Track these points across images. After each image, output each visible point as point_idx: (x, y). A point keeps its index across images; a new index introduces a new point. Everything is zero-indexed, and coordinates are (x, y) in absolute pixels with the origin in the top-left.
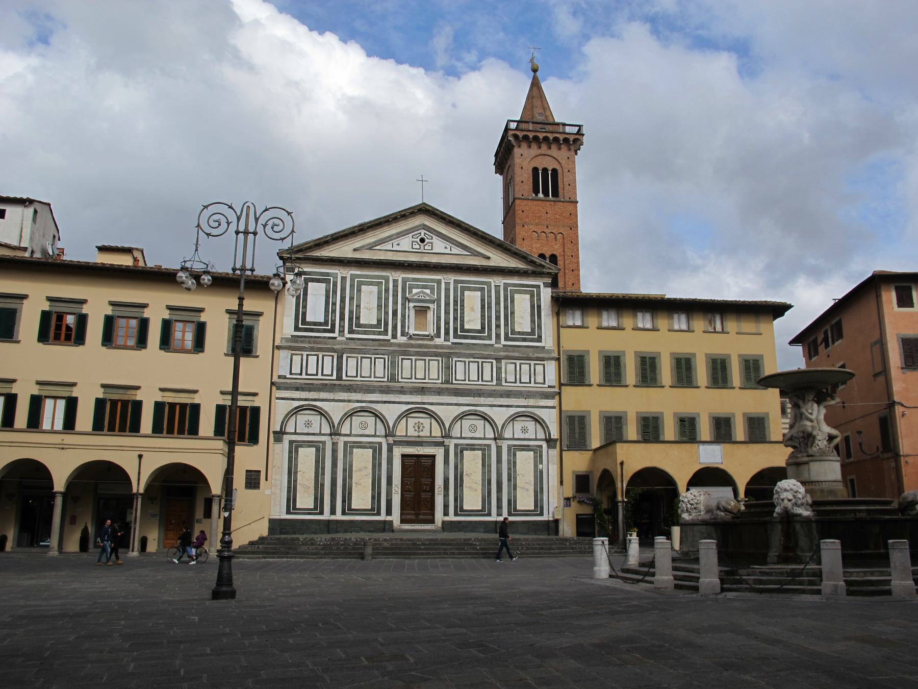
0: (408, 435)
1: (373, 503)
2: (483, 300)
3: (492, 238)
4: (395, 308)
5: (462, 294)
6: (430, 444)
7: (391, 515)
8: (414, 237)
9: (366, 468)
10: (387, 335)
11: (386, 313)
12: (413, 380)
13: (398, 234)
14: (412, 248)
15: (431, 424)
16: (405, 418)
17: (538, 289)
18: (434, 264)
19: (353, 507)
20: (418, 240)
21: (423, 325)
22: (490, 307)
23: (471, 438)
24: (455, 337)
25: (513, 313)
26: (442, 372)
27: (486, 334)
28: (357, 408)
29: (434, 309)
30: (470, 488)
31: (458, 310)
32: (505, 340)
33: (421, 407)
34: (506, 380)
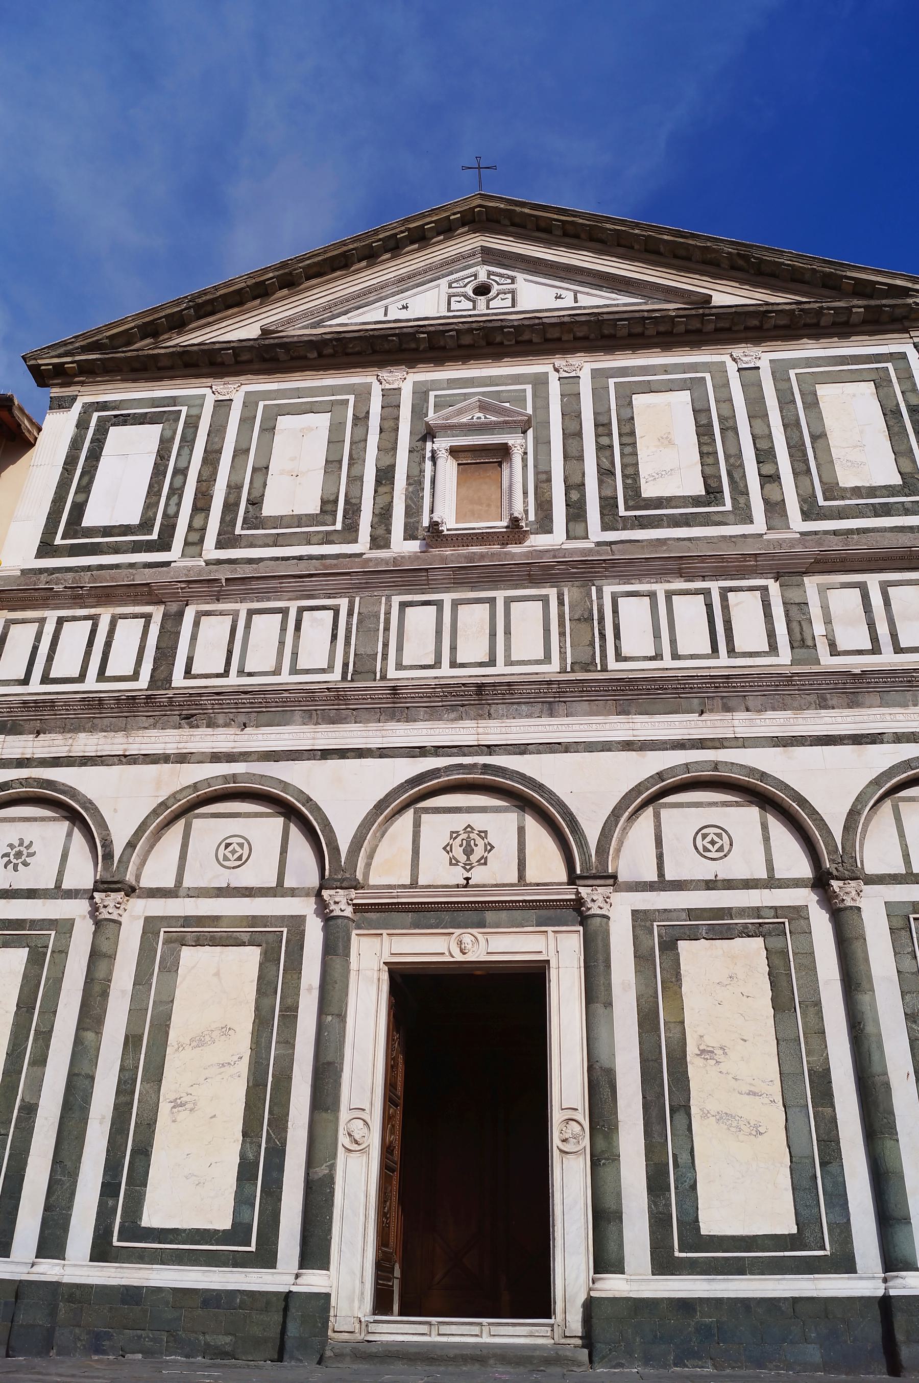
0: (421, 882)
1: (242, 1200)
2: (700, 412)
3: (709, 244)
4: (387, 462)
5: (626, 402)
6: (517, 914)
7: (327, 1268)
8: (453, 285)
9: (226, 1030)
10: (356, 541)
11: (356, 480)
12: (445, 670)
13: (401, 280)
14: (449, 310)
15: (521, 831)
16: (409, 814)
17: (901, 364)
18: (516, 323)
19: (150, 1219)
20: (469, 290)
21: (489, 505)
22: (729, 427)
23: (710, 885)
24: (605, 527)
25: (819, 437)
26: (562, 634)
27: (728, 506)
28: (208, 782)
29: (525, 453)
30: (723, 1117)
31: (611, 447)
32: (807, 515)
33: (475, 765)
34: (832, 645)
